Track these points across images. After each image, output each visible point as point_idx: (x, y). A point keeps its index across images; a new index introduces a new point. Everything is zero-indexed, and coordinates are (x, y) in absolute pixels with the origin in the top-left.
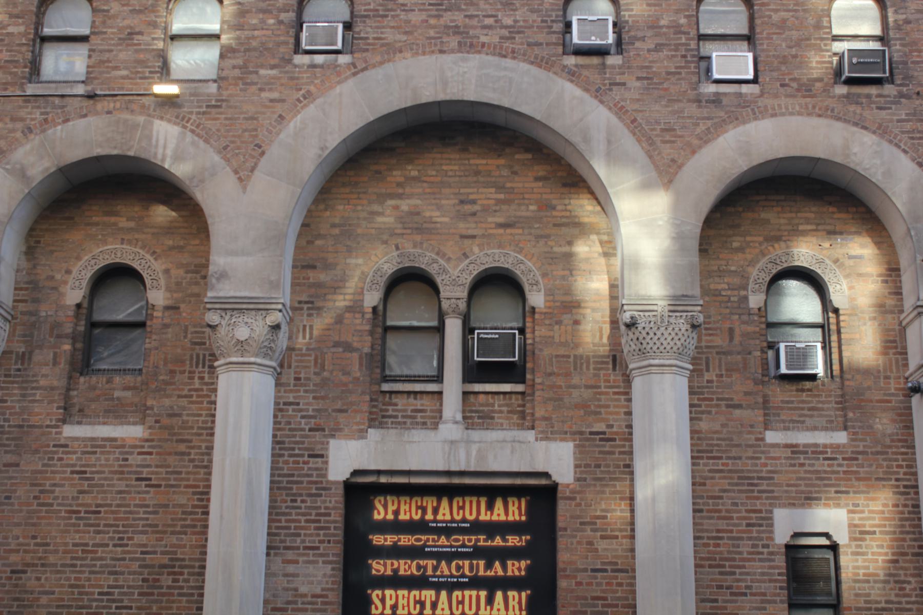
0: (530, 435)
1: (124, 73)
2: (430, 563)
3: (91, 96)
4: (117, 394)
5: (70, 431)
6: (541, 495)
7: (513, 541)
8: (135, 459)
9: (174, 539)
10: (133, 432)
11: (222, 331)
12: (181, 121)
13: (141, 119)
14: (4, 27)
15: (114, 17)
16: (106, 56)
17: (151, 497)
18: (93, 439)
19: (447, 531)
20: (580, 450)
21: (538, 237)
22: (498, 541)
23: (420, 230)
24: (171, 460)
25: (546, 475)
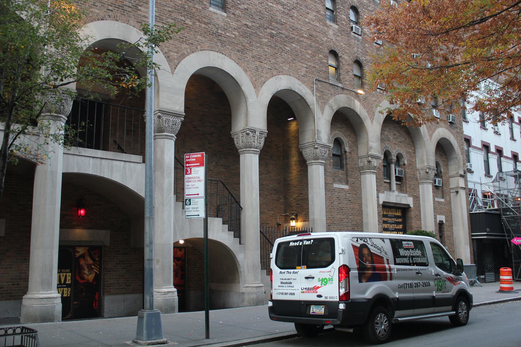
0: (406, 195)
1: (348, 83)
2: (389, 225)
3: (343, 89)
4: (340, 176)
5: (336, 186)
6: (405, 209)
7: (400, 220)
8: (348, 195)
9: (356, 217)
10: (346, 187)
11: (373, 163)
12: (359, 100)
13: (353, 98)
14: (323, 59)
15: (344, 65)
16: (344, 76)
17: (351, 206)
18: (339, 188)
19: (391, 217)
20: (414, 200)
21: (405, 146)
22: (398, 220)
23: (388, 141)
24: (354, 195)
25: (409, 205)
